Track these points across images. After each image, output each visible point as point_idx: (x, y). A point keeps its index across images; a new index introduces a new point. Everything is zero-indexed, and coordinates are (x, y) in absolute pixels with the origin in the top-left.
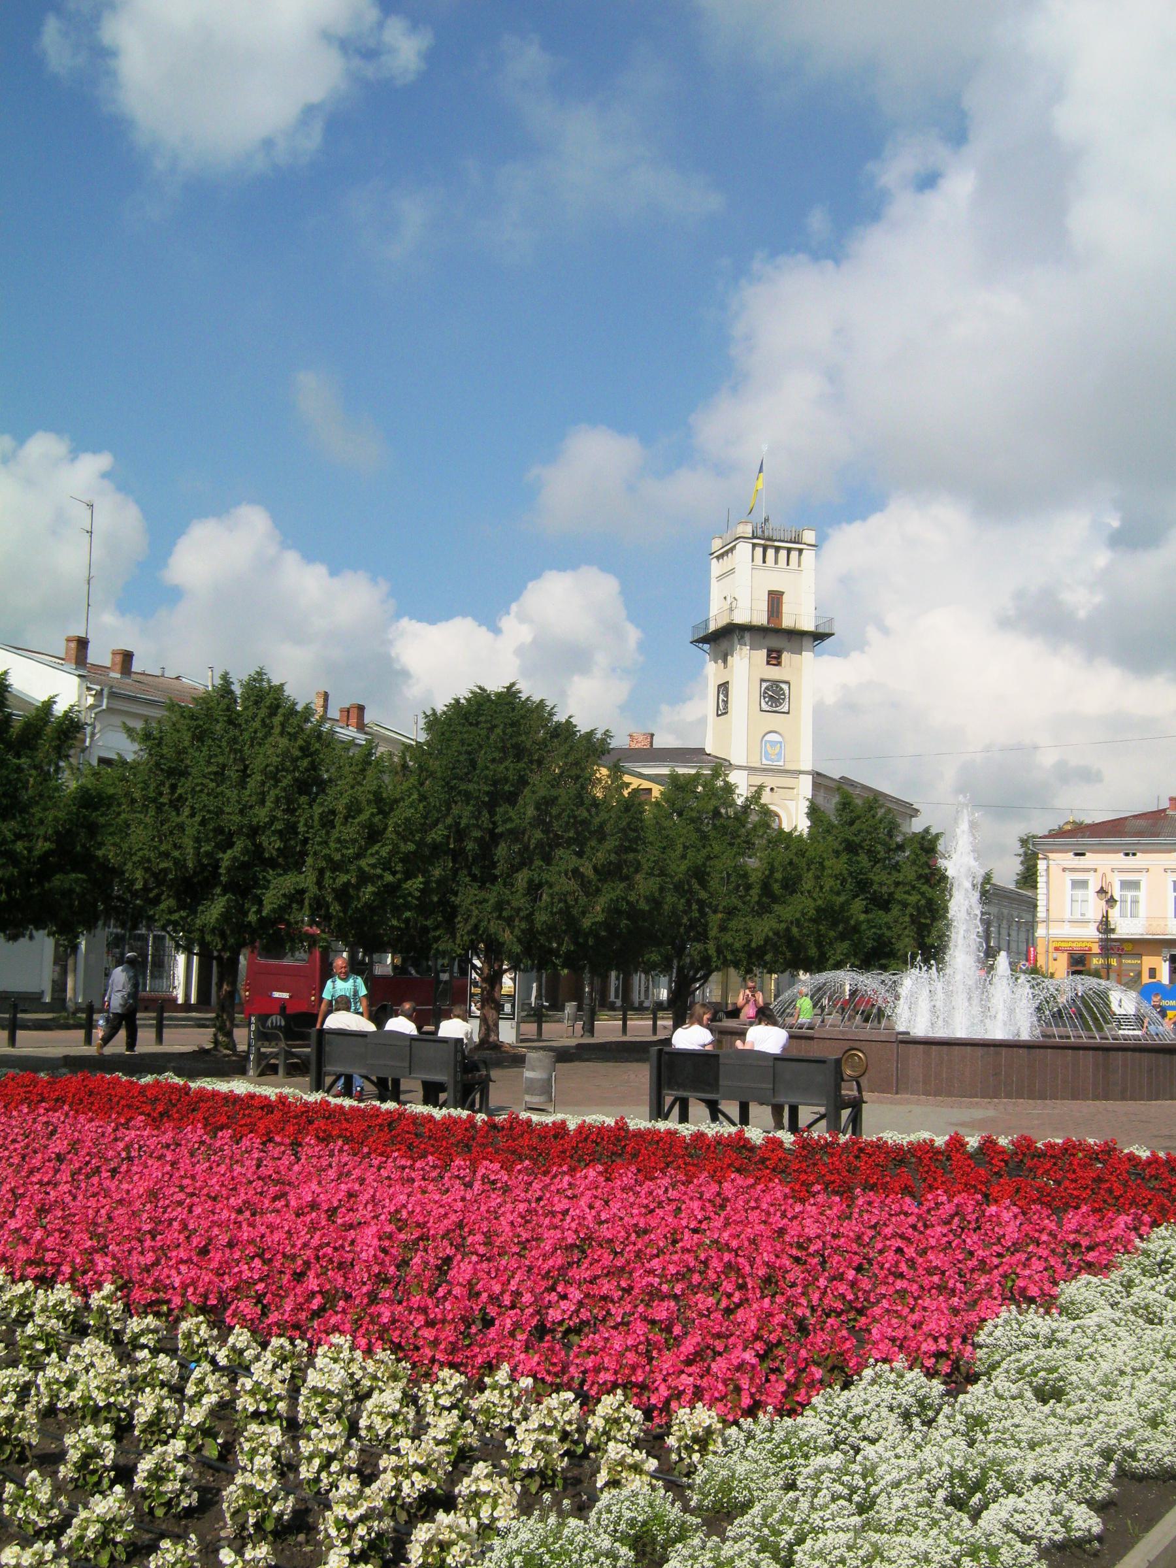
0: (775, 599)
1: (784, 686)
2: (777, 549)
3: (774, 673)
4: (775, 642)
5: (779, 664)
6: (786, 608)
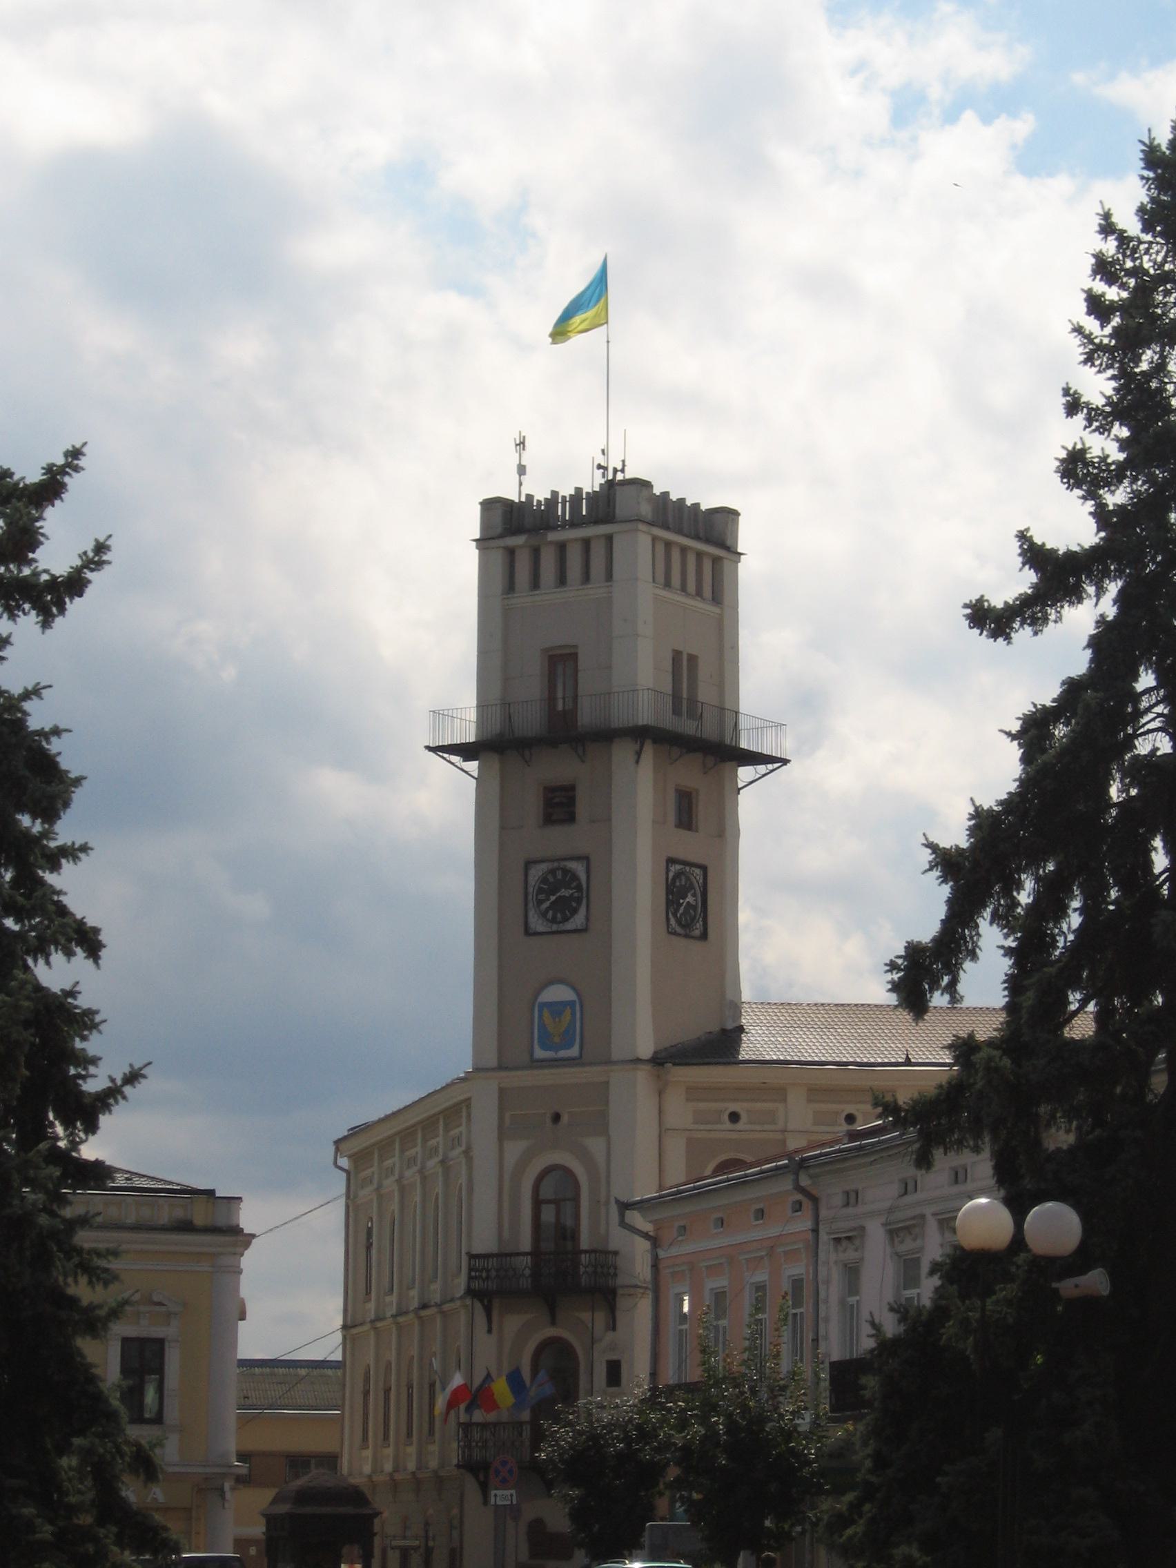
0: (561, 663)
1: (578, 868)
2: (562, 547)
3: (560, 840)
4: (558, 767)
5: (571, 818)
6: (587, 684)
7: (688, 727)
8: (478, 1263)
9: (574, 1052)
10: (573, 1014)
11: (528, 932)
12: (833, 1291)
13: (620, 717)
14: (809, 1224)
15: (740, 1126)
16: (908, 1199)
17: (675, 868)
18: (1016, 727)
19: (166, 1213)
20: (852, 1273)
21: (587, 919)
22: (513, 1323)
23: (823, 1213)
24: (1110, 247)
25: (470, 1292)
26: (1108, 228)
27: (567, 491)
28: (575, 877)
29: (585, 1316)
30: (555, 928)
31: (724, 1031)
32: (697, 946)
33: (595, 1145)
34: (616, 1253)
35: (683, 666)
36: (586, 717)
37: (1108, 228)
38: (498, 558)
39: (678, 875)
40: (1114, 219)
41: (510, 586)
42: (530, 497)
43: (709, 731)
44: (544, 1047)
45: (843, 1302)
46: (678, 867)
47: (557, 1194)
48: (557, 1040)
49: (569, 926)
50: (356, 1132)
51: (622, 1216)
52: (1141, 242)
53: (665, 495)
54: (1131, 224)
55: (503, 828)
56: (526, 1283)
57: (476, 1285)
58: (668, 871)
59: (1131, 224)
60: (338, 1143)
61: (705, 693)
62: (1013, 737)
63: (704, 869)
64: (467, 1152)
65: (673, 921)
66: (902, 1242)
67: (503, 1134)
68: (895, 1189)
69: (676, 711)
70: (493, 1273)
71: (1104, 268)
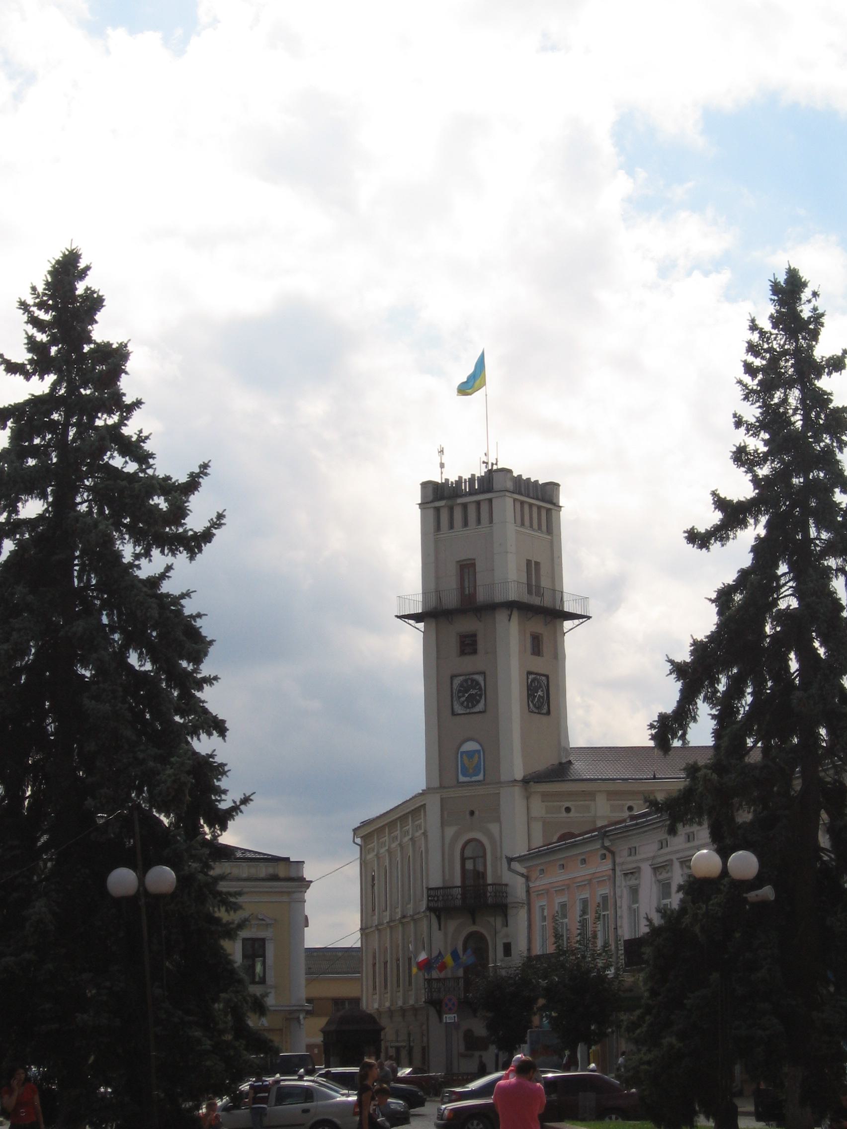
0: (467, 568)
1: (480, 679)
2: (465, 506)
3: (468, 664)
4: (466, 625)
5: (475, 652)
6: (481, 579)
7: (536, 601)
8: (432, 893)
9: (480, 777)
10: (479, 758)
11: (454, 714)
12: (624, 903)
13: (499, 598)
14: (610, 866)
15: (572, 814)
16: (663, 851)
17: (531, 677)
18: (714, 596)
19: (263, 870)
20: (634, 891)
21: (485, 705)
22: (452, 925)
23: (618, 860)
24: (755, 337)
25: (429, 909)
26: (754, 327)
27: (466, 476)
28: (478, 683)
29: (492, 919)
30: (468, 711)
31: (561, 764)
32: (544, 719)
33: (494, 828)
34: (506, 885)
35: (532, 568)
36: (482, 596)
37: (754, 327)
38: (431, 513)
39: (533, 681)
40: (757, 322)
41: (438, 528)
42: (447, 480)
43: (547, 602)
44: (464, 775)
45: (630, 908)
46: (533, 676)
47: (473, 856)
48: (471, 771)
49: (476, 709)
50: (365, 824)
51: (509, 864)
52: (771, 334)
53: (520, 476)
54: (767, 326)
55: (438, 658)
56: (458, 903)
57: (431, 904)
58: (528, 678)
59: (767, 326)
60: (355, 830)
61: (545, 583)
62: (713, 601)
63: (547, 677)
64: (425, 834)
65: (531, 705)
66: (660, 874)
67: (443, 824)
68: (656, 846)
69: (530, 592)
70: (441, 898)
71: (752, 349)
